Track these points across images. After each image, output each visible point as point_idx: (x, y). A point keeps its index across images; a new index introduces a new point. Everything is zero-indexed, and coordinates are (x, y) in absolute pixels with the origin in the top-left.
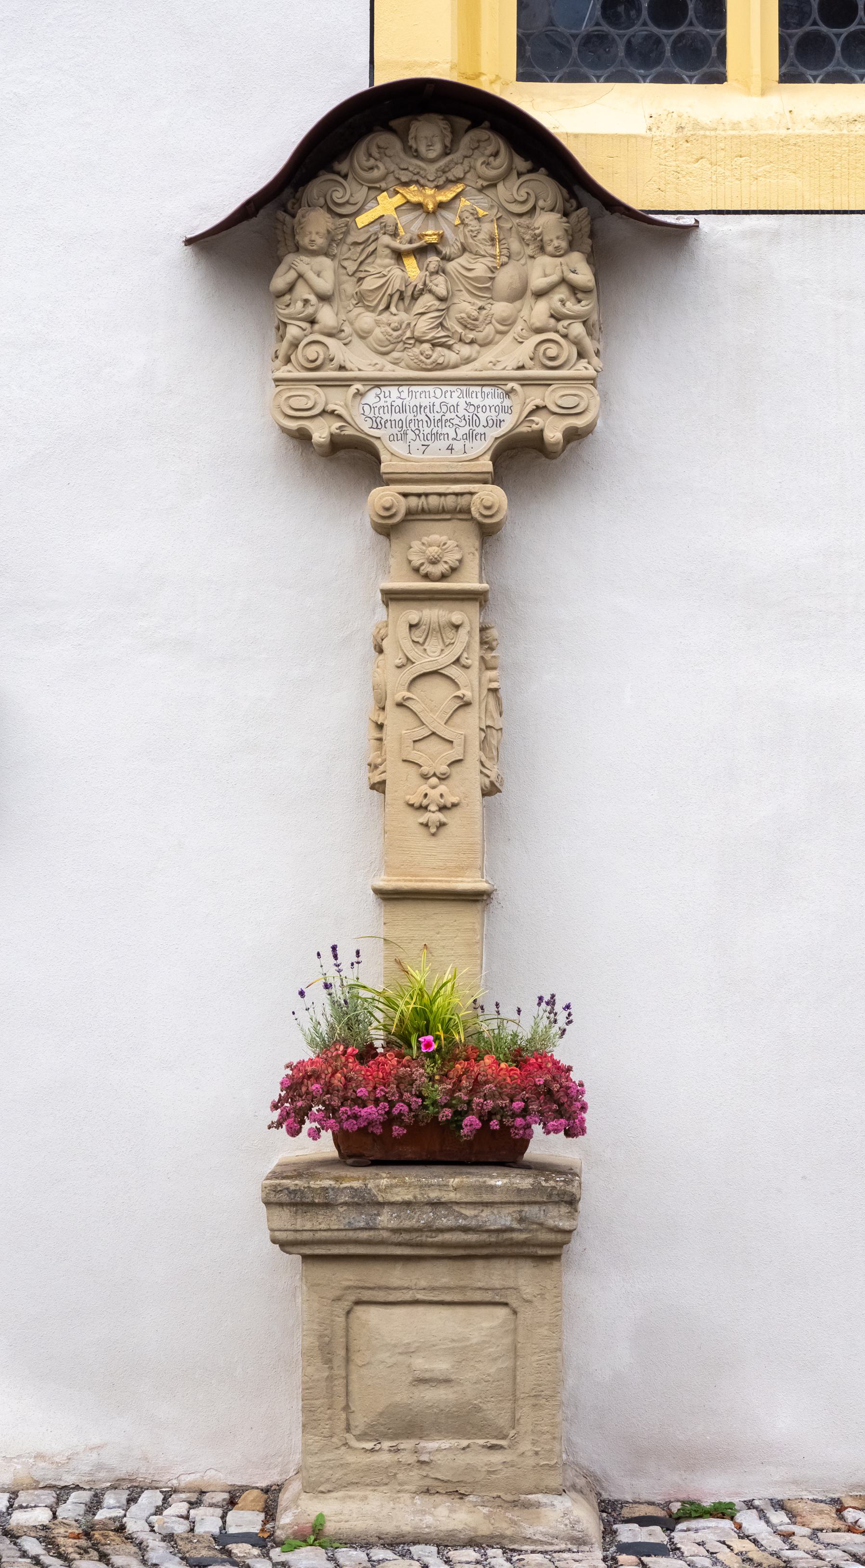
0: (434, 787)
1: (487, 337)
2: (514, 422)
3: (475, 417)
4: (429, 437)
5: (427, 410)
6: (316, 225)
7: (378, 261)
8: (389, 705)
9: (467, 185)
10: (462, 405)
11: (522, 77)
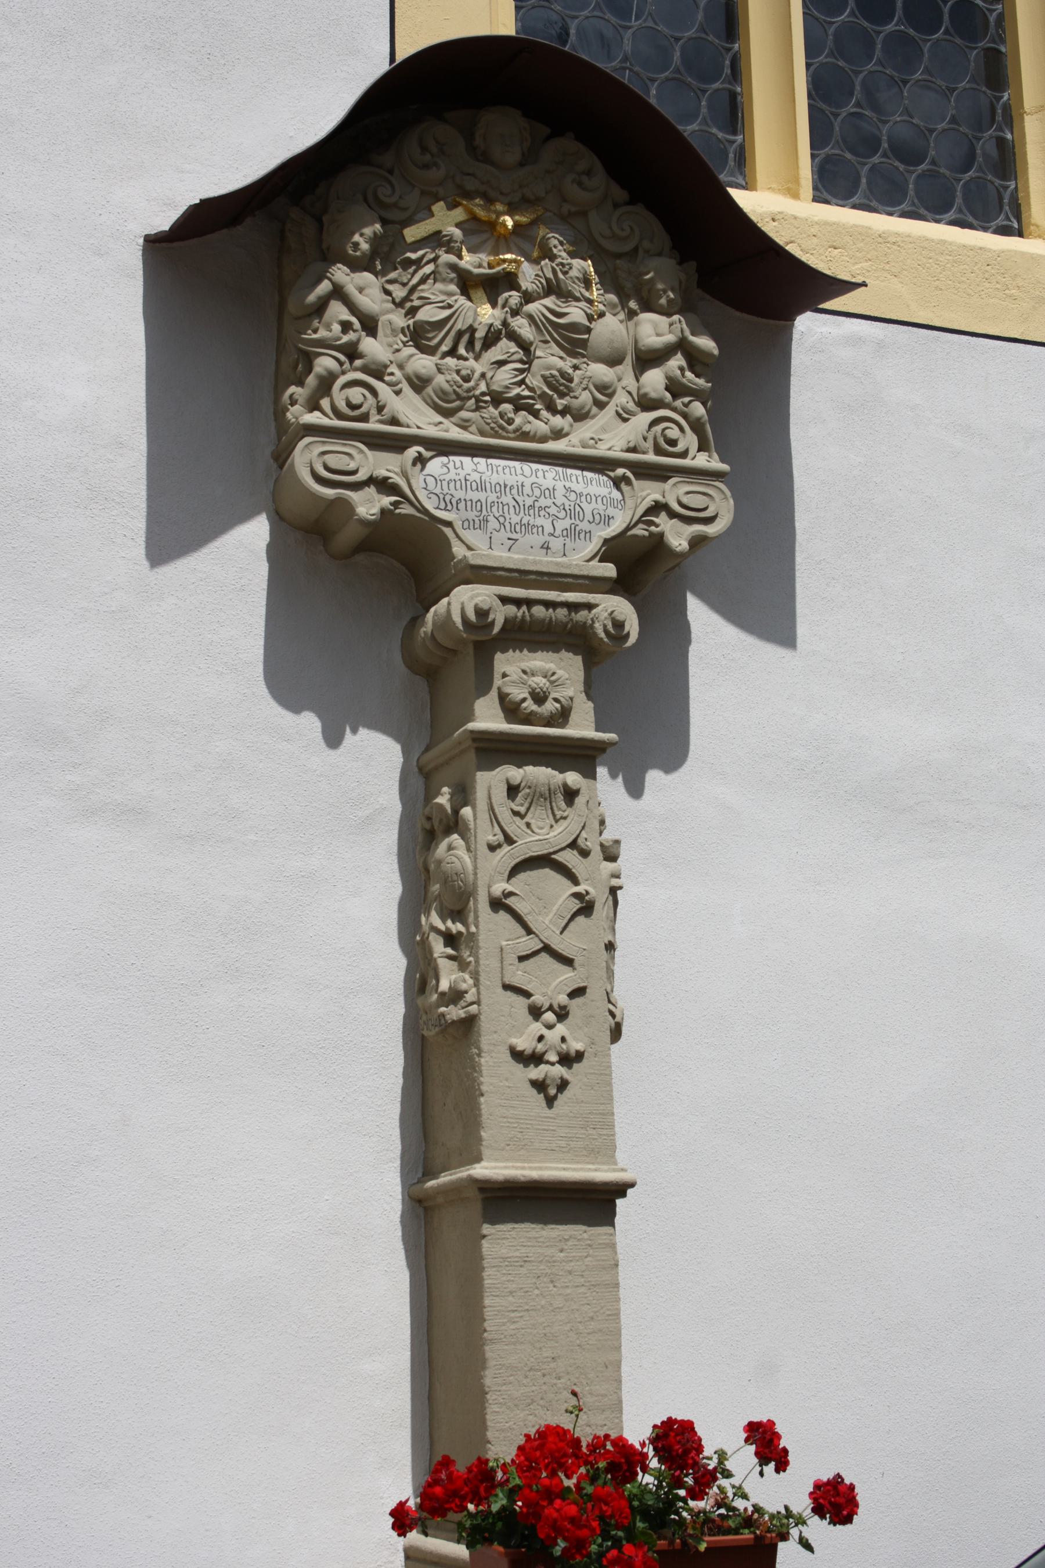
0: (550, 1027)
1: (583, 407)
2: (628, 521)
3: (578, 508)
4: (518, 528)
5: (514, 492)
9: (546, 210)
10: (560, 492)
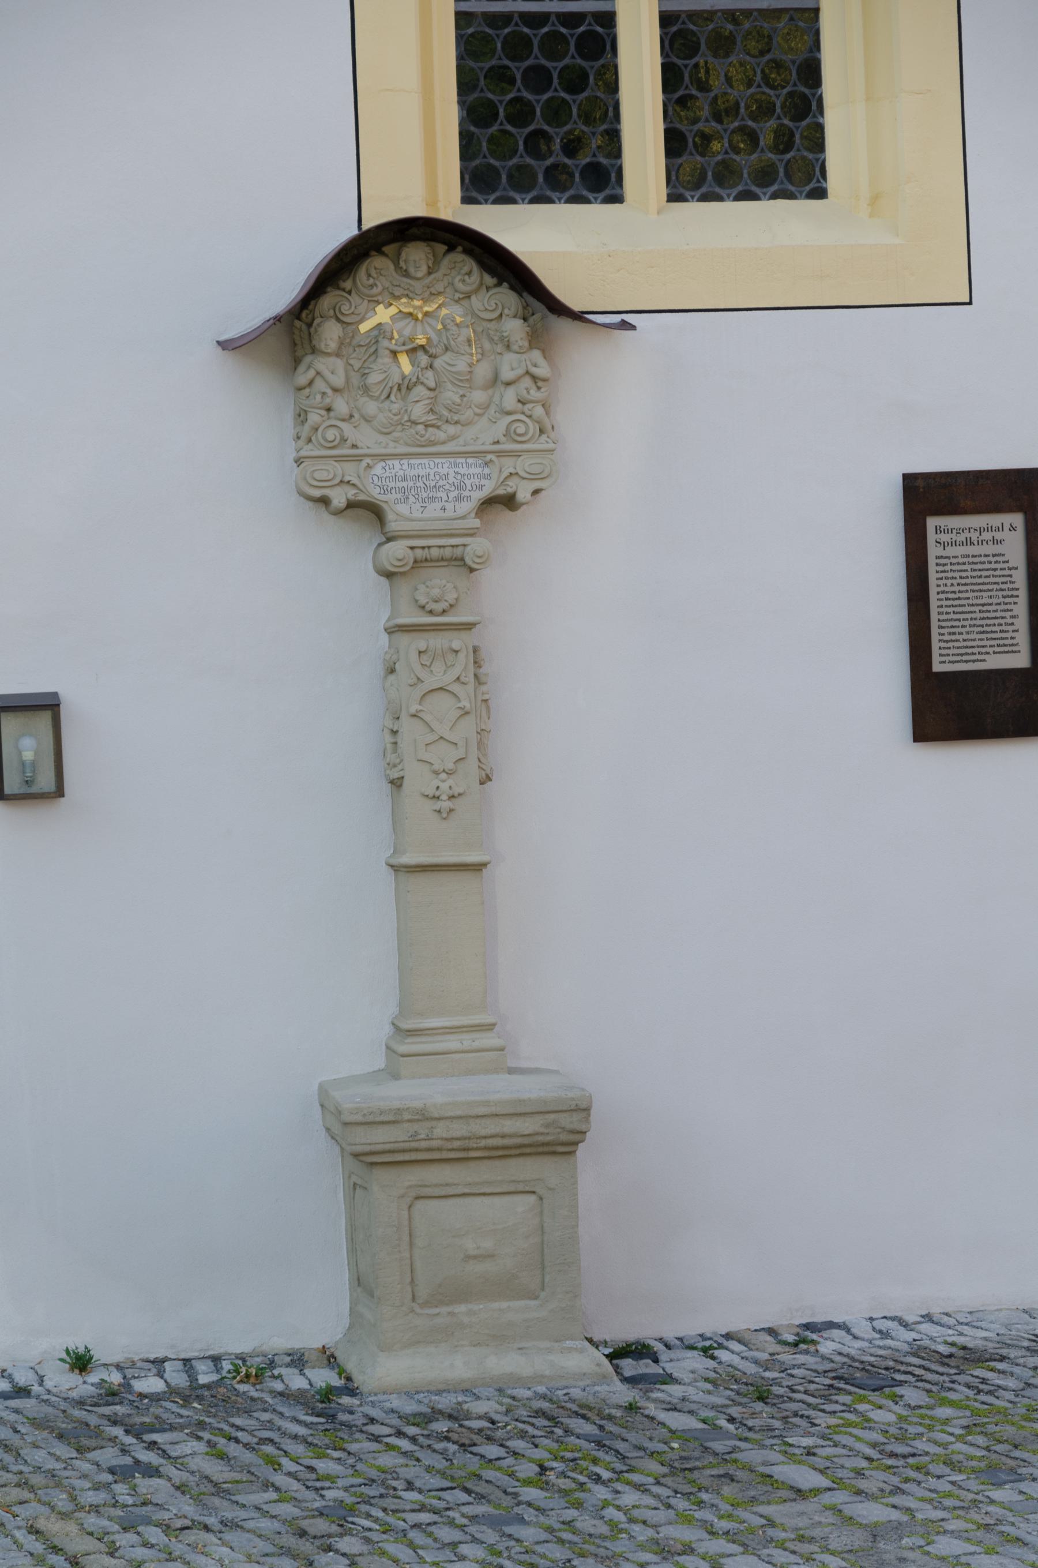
0: (444, 781)
6: (330, 333)
7: (379, 360)
8: (404, 717)
10: (452, 474)
11: (467, 200)
